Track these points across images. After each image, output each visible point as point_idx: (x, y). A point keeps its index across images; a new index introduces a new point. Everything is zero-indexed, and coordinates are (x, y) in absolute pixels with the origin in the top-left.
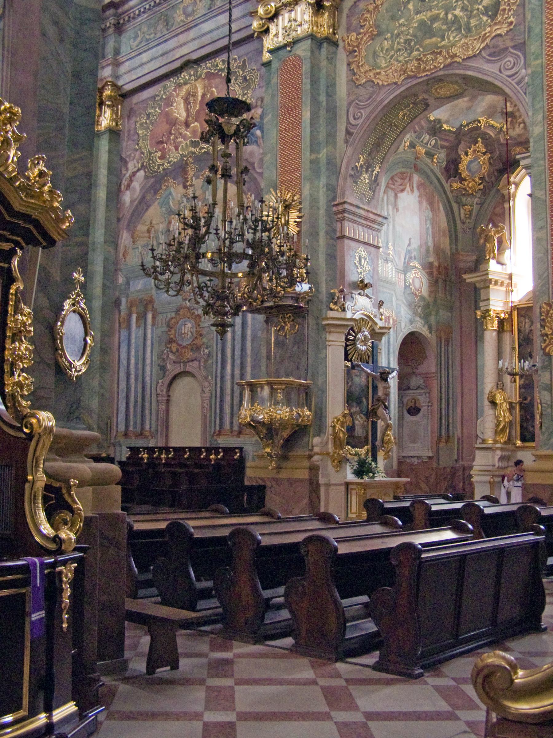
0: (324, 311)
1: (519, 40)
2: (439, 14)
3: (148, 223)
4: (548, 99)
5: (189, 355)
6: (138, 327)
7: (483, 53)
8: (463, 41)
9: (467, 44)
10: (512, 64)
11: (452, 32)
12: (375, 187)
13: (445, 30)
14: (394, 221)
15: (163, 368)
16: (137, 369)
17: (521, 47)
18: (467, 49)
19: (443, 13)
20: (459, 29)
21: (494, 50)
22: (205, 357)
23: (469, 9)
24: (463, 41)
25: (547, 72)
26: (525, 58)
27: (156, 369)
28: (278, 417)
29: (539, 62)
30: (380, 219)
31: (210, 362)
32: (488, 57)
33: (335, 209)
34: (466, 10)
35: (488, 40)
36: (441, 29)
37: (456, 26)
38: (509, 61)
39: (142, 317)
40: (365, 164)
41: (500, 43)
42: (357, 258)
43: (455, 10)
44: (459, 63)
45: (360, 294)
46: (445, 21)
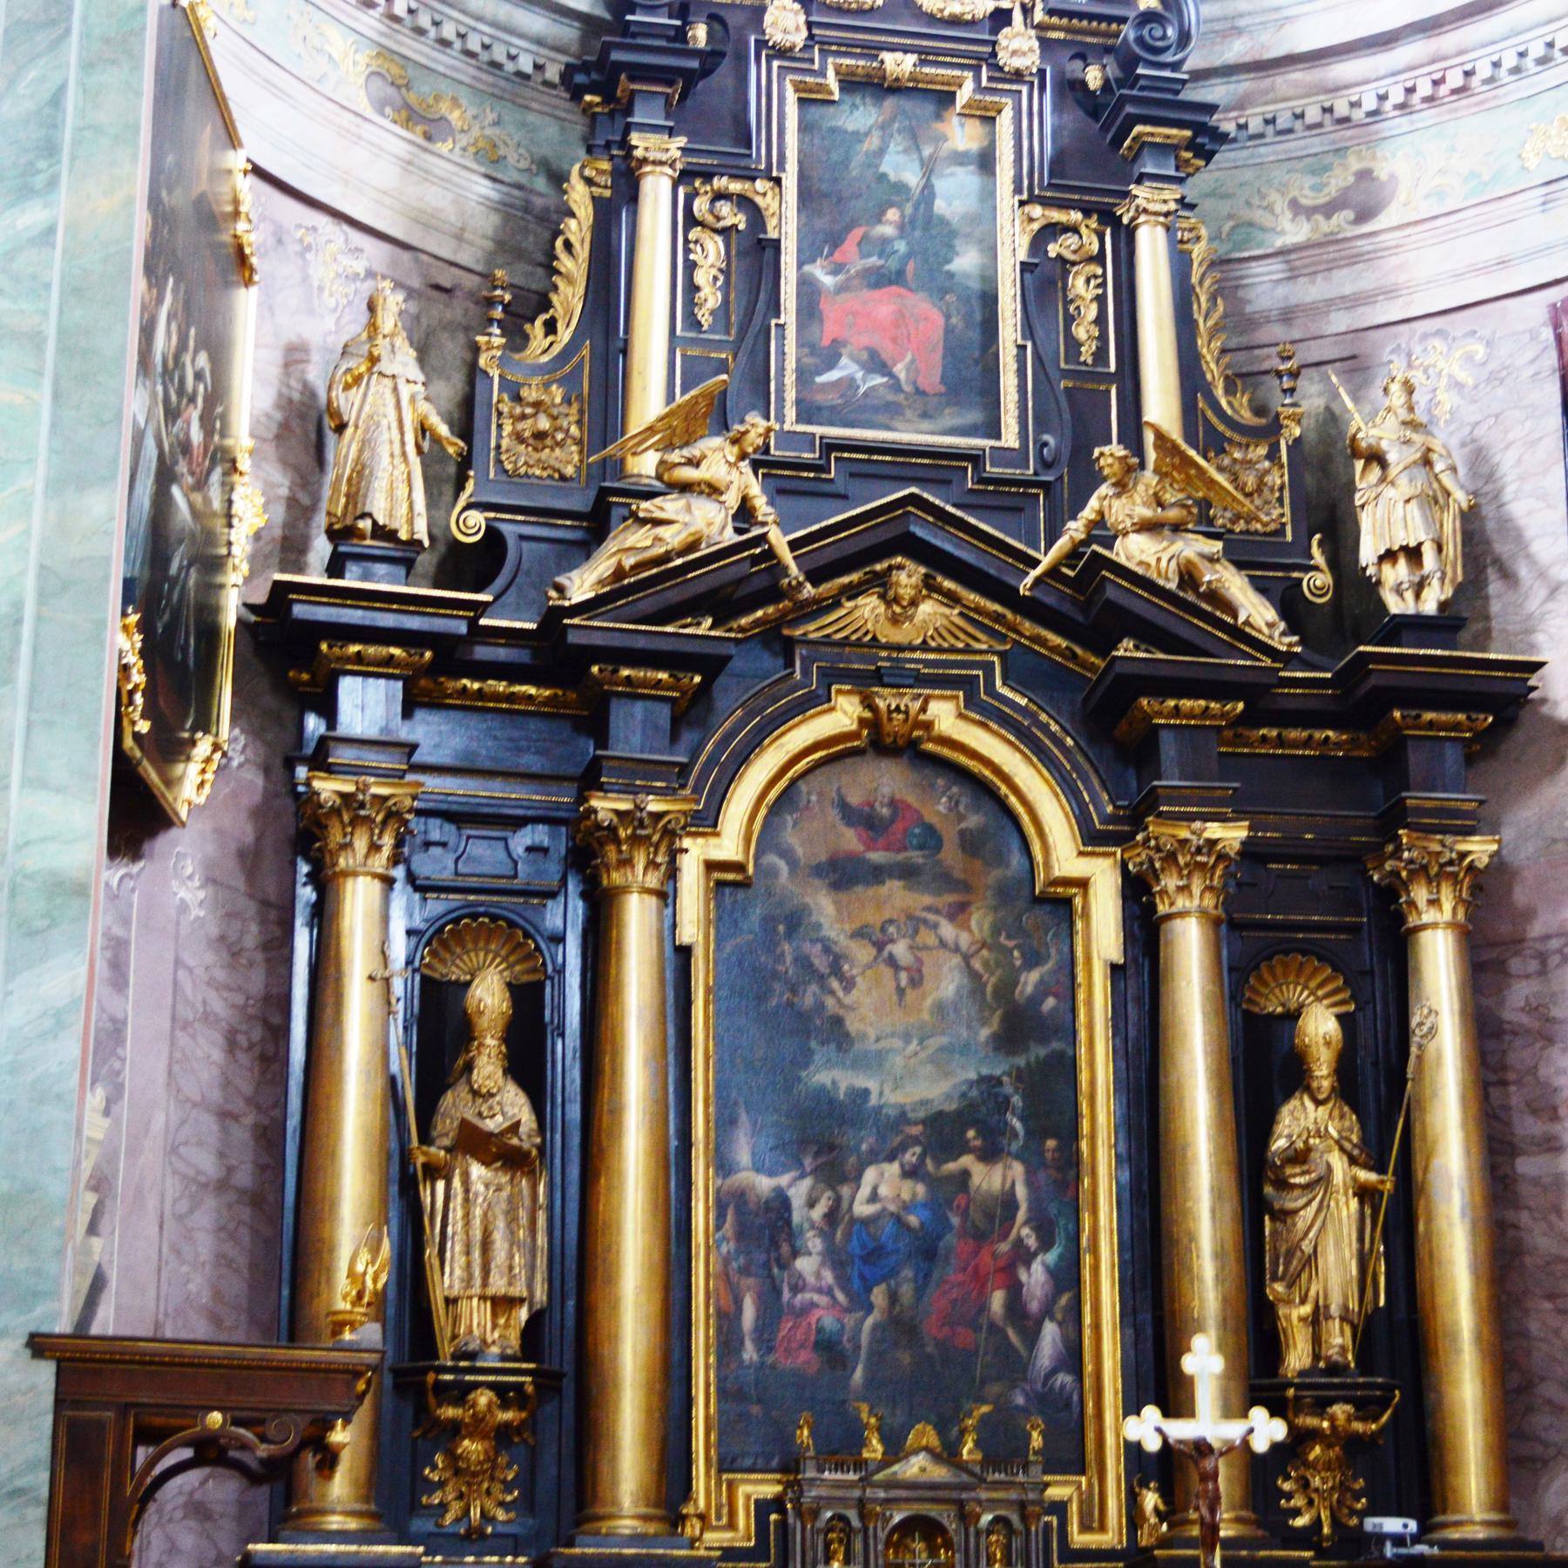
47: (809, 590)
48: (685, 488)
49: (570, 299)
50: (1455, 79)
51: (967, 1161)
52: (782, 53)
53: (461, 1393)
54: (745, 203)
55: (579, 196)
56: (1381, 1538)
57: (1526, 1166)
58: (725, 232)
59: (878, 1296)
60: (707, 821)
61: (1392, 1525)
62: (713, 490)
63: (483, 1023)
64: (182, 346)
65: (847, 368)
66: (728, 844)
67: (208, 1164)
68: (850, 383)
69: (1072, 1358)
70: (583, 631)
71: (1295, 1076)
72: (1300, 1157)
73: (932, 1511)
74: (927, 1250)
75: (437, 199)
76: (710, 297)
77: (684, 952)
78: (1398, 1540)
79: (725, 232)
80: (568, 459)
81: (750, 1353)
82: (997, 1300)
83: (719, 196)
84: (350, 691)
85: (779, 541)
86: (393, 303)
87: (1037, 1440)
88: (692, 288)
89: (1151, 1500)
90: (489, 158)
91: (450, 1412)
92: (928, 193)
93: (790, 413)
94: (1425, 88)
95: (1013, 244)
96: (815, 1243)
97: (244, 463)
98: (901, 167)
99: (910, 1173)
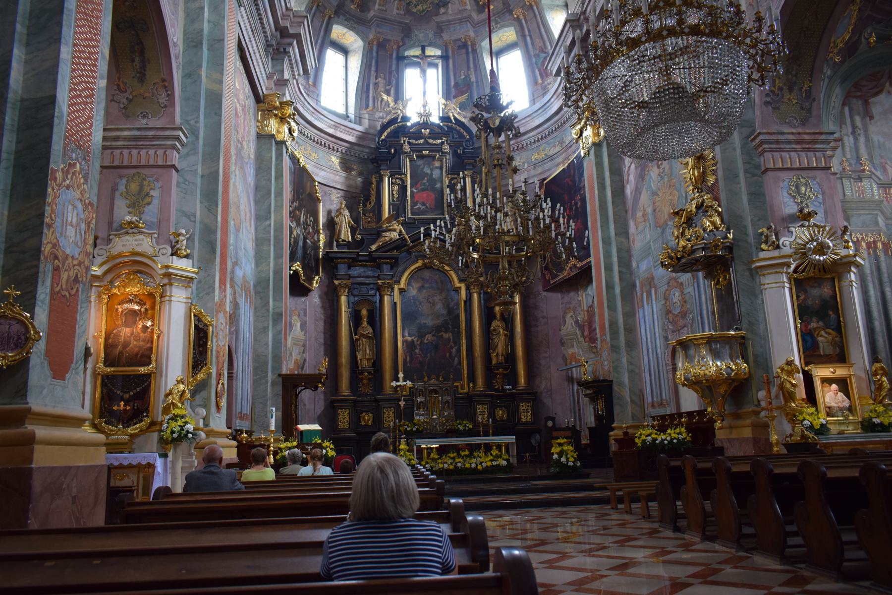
0: (754, 254)
3: (642, 209)
5: (681, 322)
6: (648, 303)
12: (811, 104)
14: (866, 130)
15: (666, 338)
16: (652, 343)
22: (690, 322)
27: (662, 339)
28: (702, 372)
30: (823, 137)
31: (694, 326)
33: (754, 144)
39: (649, 294)
40: (785, 84)
42: (793, 188)
45: (802, 226)
47: (411, 244)
48: (390, 230)
49: (373, 198)
50: (520, 146)
51: (442, 333)
52: (406, 153)
53: (362, 373)
54: (401, 179)
55: (374, 180)
56: (506, 389)
57: (533, 329)
58: (398, 185)
59: (429, 355)
60: (398, 282)
61: (508, 387)
62: (394, 230)
63: (363, 317)
64: (307, 217)
65: (419, 205)
66: (402, 285)
67: (322, 341)
68: (419, 208)
69: (460, 363)
70: (375, 255)
71: (495, 317)
72: (495, 330)
73: (436, 388)
74: (436, 347)
75: (352, 182)
76: (396, 196)
77: (395, 303)
78: (509, 389)
79: (398, 185)
80: (374, 225)
81: (408, 365)
82: (448, 355)
83: (397, 178)
84: (339, 266)
85: (406, 236)
86: (344, 202)
87: (452, 376)
88: (393, 194)
89: (471, 385)
90: (360, 174)
91: (361, 376)
92: (432, 174)
93: (410, 214)
94: (516, 148)
95: (446, 181)
96: (418, 347)
97: (321, 232)
98: (427, 170)
99: (433, 336)
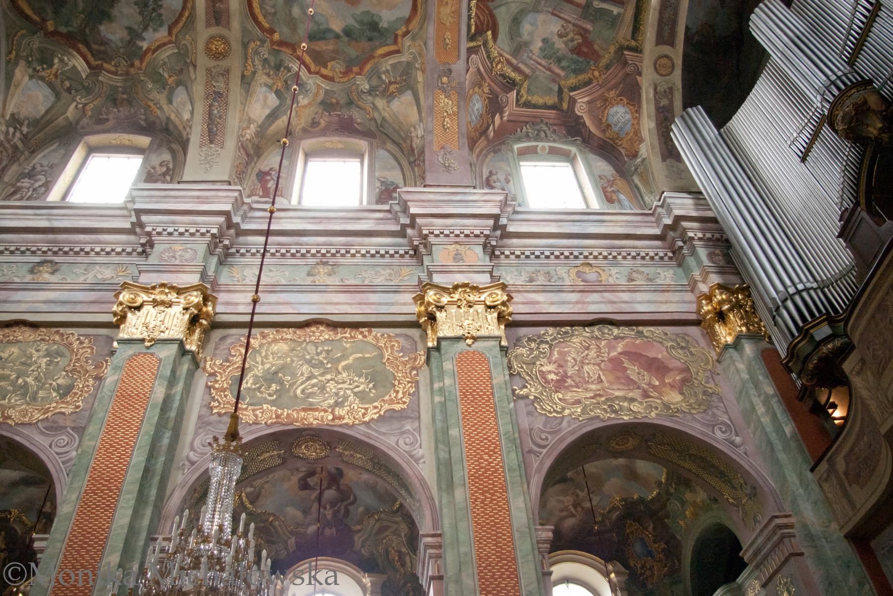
1: (82, 422)
2: (10, 375)
4: (89, 481)
7: (40, 424)
8: (24, 407)
9: (27, 411)
10: (65, 443)
11: (16, 395)
13: (10, 391)
17: (81, 430)
18: (24, 416)
19: (15, 376)
20: (24, 395)
21: (53, 425)
23: (43, 381)
24: (24, 407)
25: (97, 455)
26: (80, 441)
29: (93, 443)
32: (43, 430)
34: (39, 381)
35: (50, 414)
36: (6, 389)
37: (22, 391)
38: (64, 440)
41: (61, 422)
43: (28, 377)
44: (11, 426)
46: (14, 383)
